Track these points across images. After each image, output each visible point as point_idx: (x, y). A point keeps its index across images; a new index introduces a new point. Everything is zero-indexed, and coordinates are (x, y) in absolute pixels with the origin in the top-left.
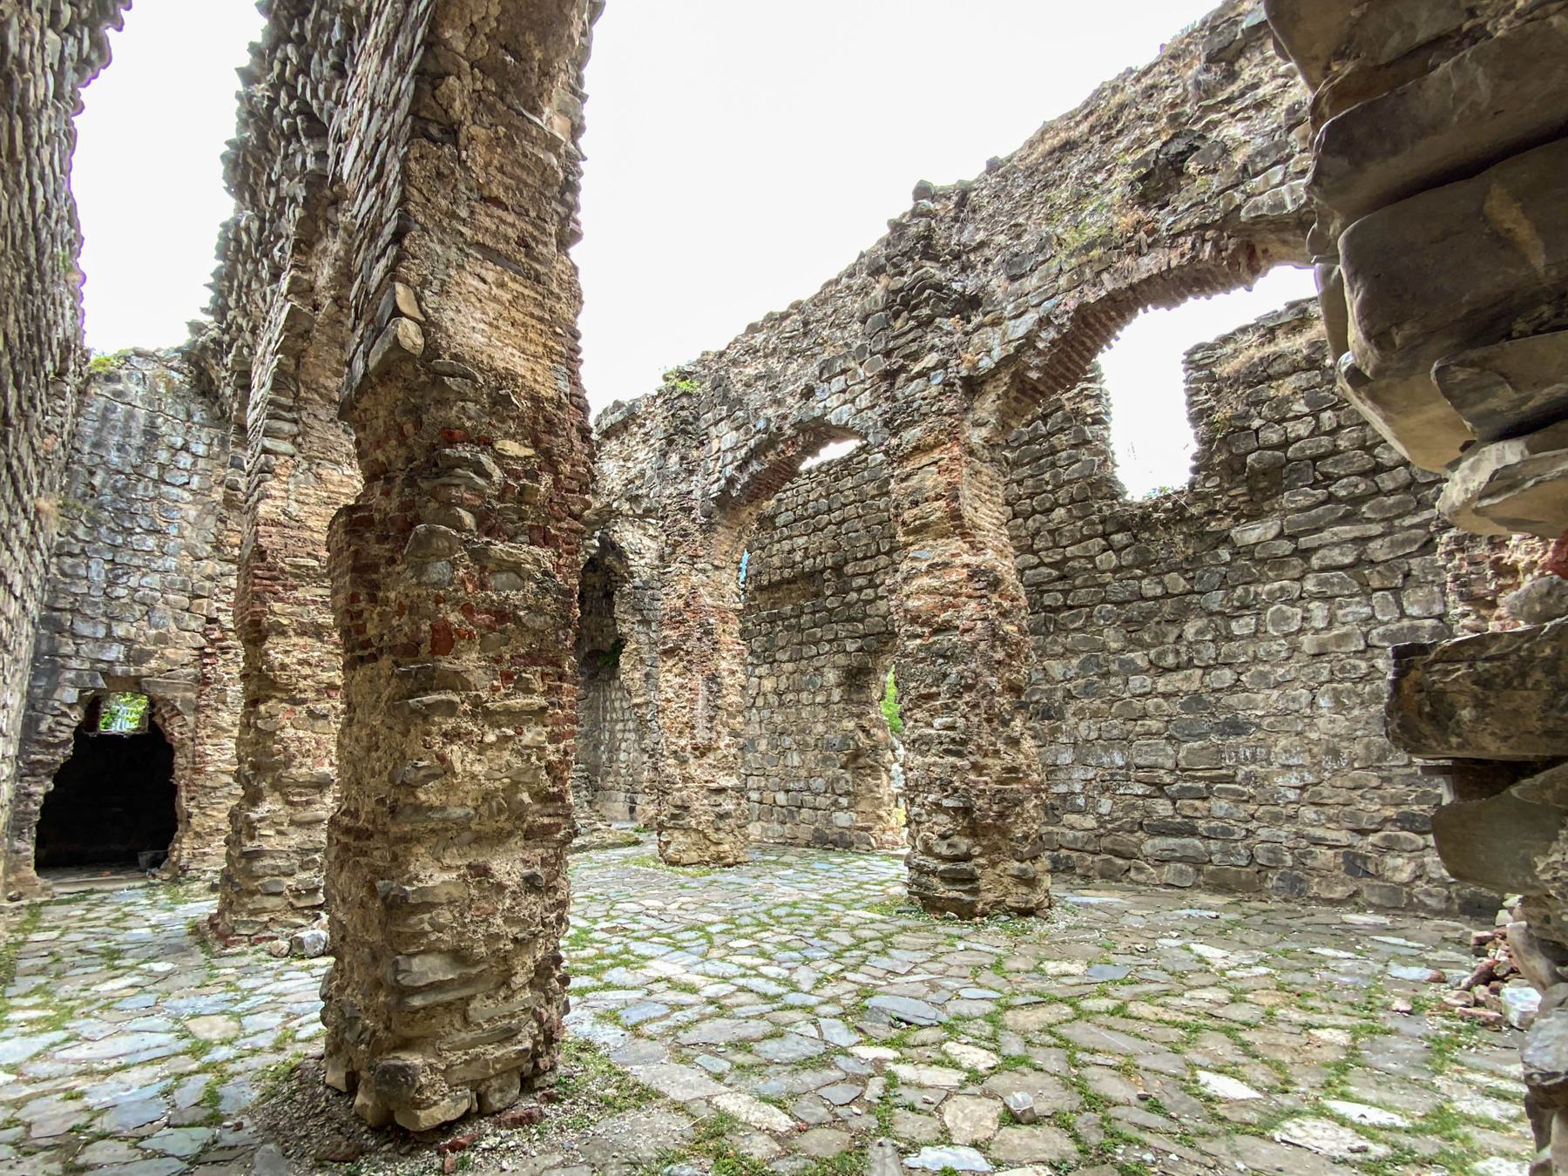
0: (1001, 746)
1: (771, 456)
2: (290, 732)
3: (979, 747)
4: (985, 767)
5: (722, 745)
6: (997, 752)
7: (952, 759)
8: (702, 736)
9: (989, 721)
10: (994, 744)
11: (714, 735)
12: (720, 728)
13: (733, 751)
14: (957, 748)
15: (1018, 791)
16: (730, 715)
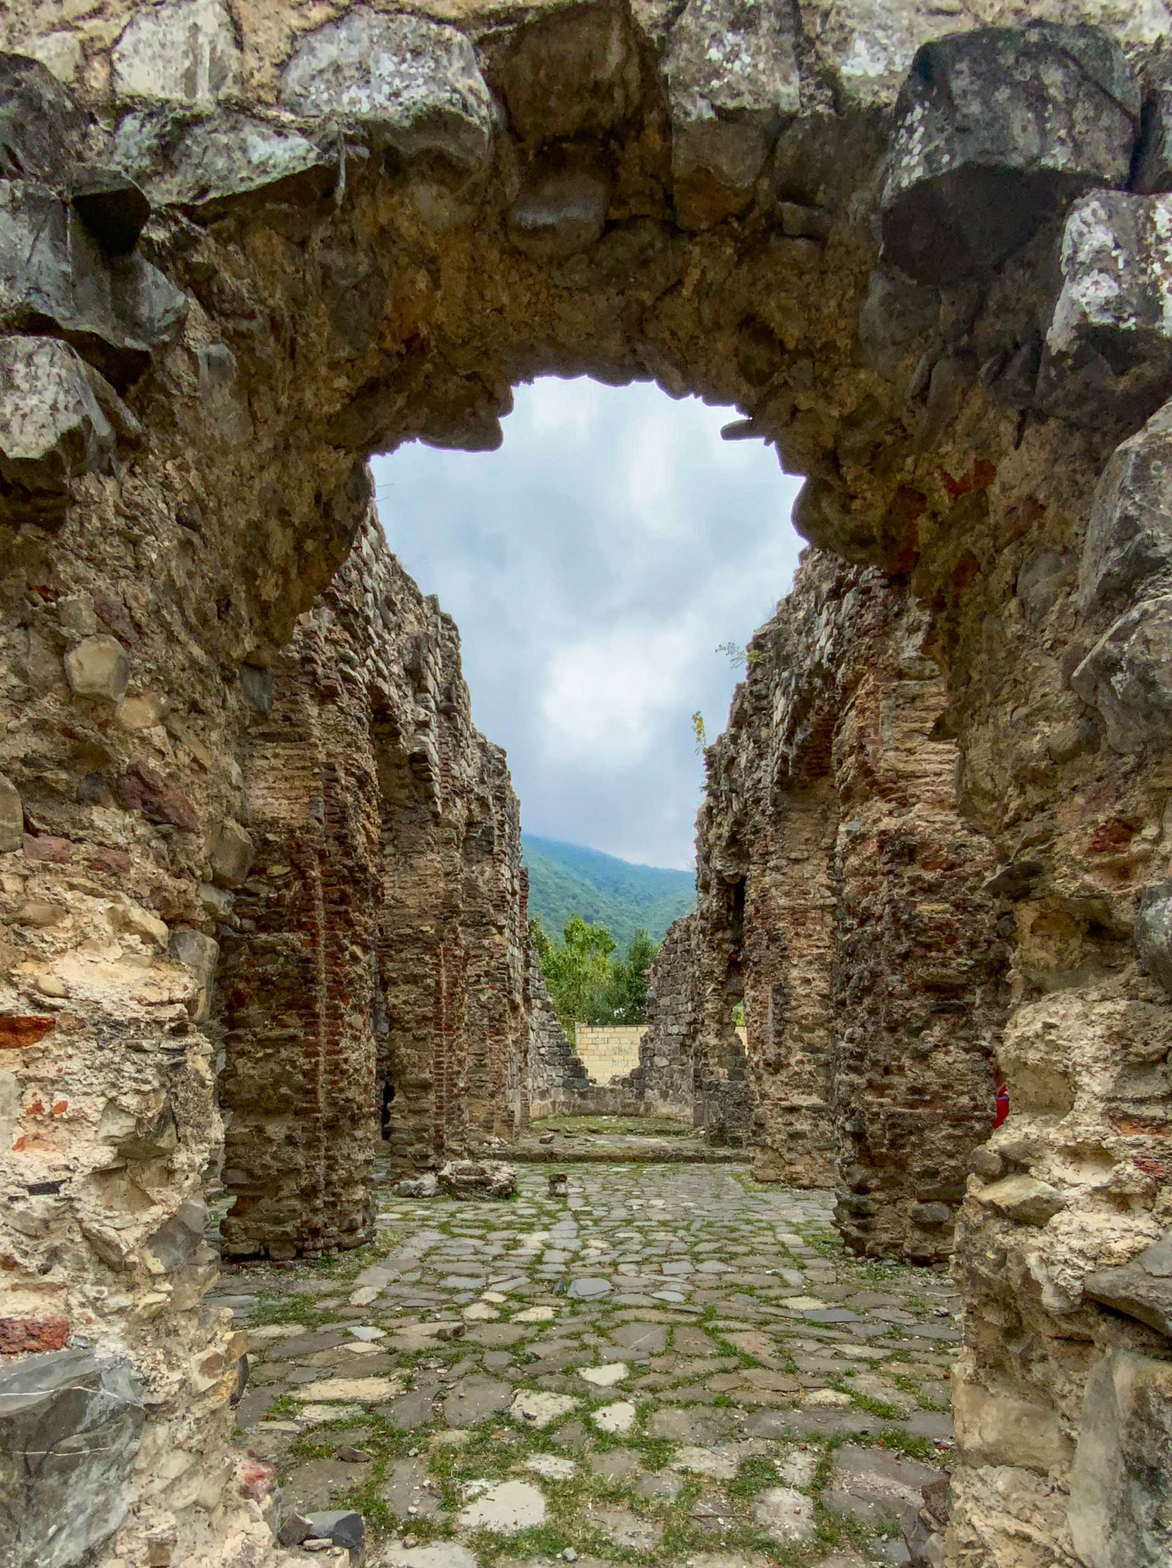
0: (906, 1062)
1: (813, 717)
2: (403, 1050)
3: (875, 1063)
4: (890, 1086)
5: (793, 1061)
6: (901, 1069)
7: (853, 1077)
8: (771, 1051)
9: (892, 1030)
10: (898, 1059)
11: (783, 1051)
12: (790, 1043)
13: (808, 1068)
14: (857, 1060)
15: (919, 1117)
16: (804, 1028)
